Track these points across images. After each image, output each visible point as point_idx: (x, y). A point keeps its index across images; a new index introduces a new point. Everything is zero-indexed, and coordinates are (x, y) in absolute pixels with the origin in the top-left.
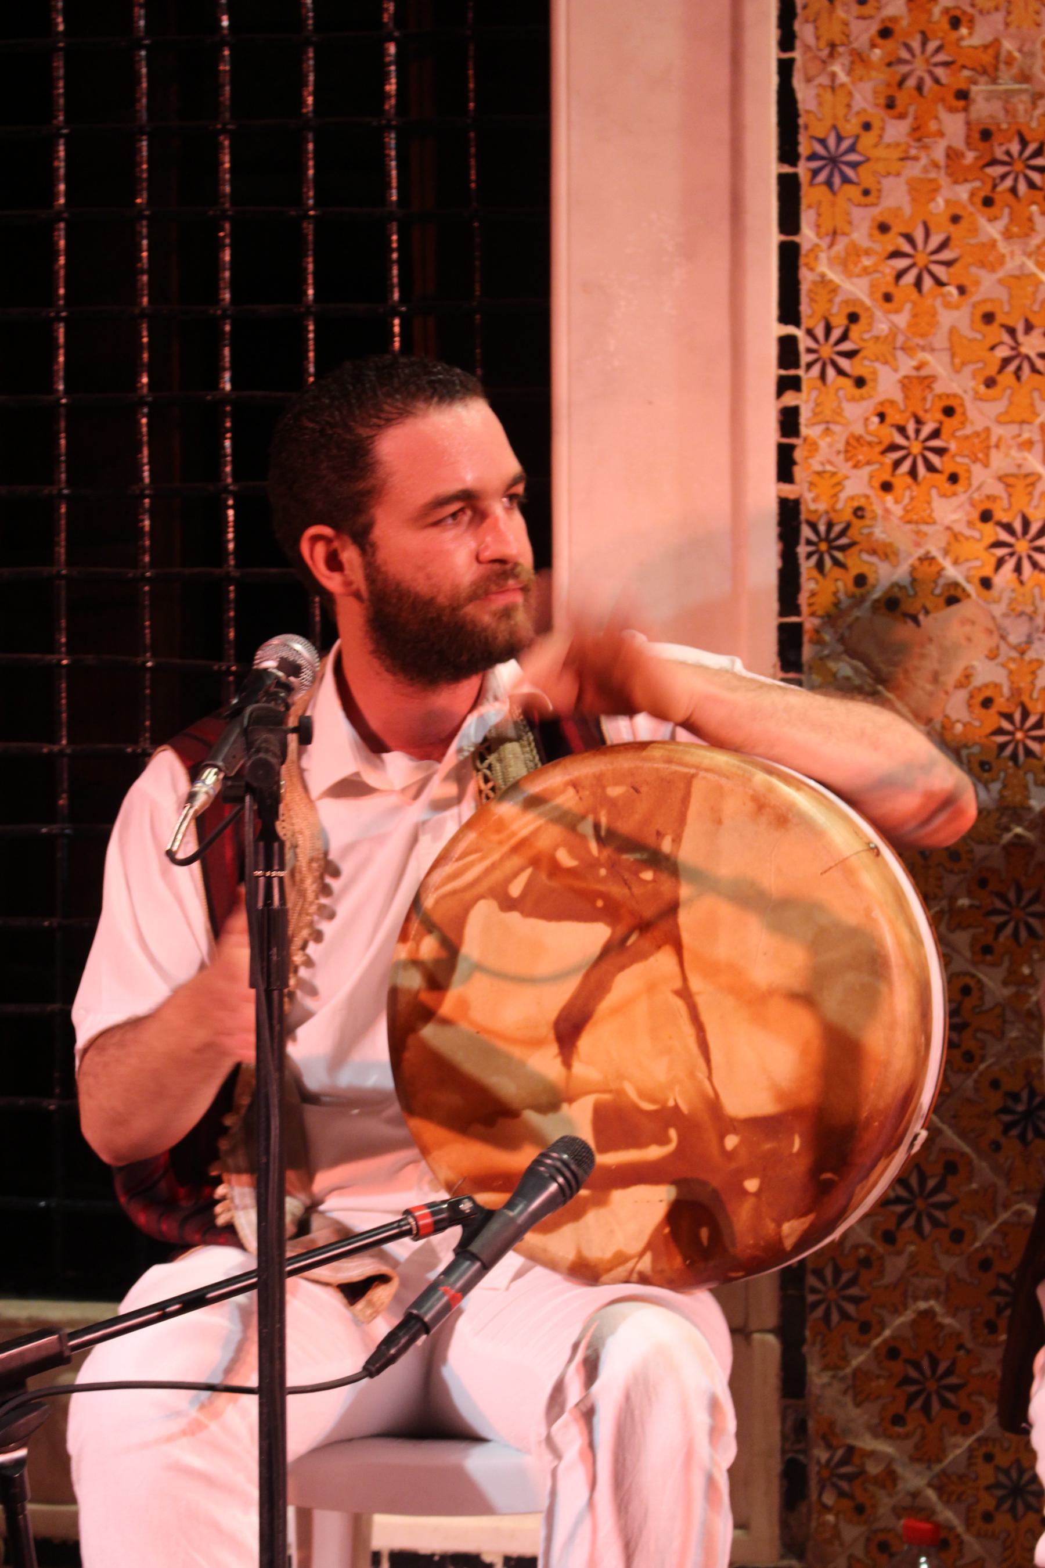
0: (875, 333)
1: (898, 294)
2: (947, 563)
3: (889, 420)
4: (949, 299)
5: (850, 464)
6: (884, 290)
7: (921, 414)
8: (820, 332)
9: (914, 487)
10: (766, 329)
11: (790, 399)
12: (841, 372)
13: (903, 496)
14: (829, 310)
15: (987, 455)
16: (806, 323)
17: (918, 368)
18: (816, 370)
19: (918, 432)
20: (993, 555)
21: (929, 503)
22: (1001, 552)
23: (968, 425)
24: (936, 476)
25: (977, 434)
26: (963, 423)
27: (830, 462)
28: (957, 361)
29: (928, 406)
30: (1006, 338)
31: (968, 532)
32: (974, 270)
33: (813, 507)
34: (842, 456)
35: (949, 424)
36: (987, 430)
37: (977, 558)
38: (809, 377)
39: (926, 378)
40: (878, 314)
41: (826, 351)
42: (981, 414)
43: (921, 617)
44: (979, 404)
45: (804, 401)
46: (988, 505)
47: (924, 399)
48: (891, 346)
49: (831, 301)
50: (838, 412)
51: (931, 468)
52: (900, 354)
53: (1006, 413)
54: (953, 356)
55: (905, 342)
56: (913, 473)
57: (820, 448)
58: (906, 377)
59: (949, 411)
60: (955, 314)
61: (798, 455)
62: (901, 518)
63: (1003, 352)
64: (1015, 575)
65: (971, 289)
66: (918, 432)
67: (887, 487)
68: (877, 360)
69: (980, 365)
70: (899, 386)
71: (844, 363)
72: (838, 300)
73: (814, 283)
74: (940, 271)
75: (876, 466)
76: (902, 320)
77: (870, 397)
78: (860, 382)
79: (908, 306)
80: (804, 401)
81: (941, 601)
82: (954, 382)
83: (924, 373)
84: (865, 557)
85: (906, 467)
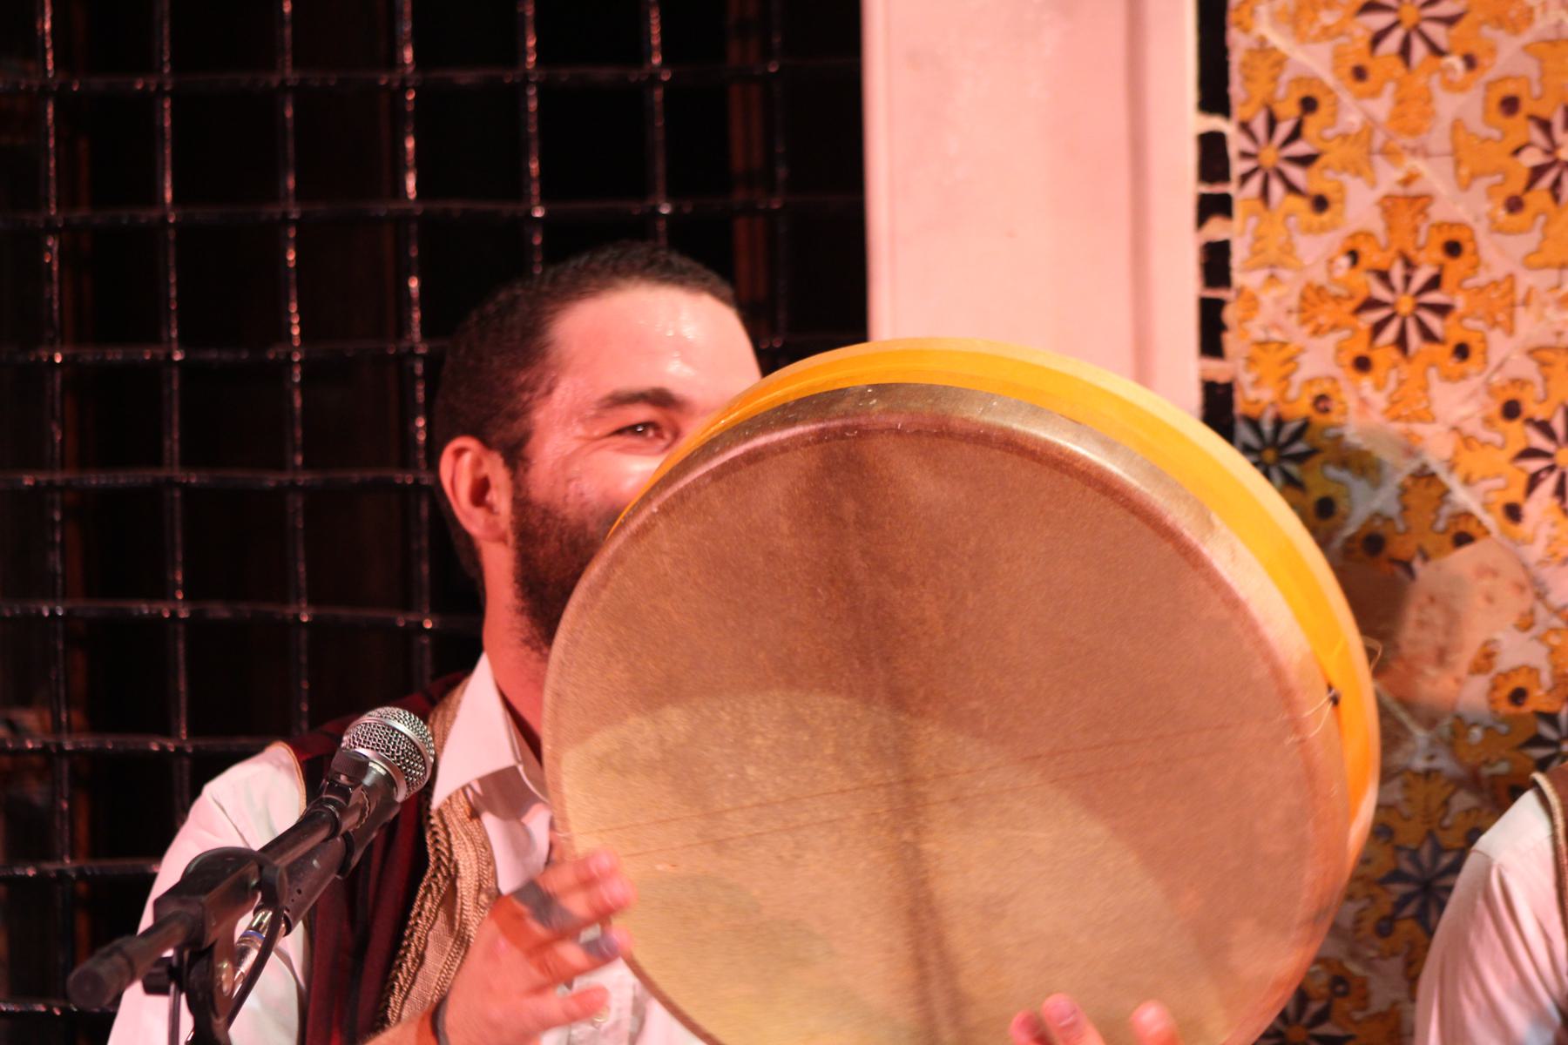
0: (1340, 128)
1: (1375, 70)
2: (1453, 482)
3: (1365, 262)
4: (1450, 76)
5: (1307, 329)
6: (1353, 61)
7: (1411, 252)
8: (1259, 126)
9: (1404, 367)
10: (1180, 121)
11: (1217, 229)
12: (1291, 188)
13: (1386, 378)
14: (1272, 93)
15: (1511, 317)
16: (1238, 111)
17: (1407, 182)
18: (1254, 184)
19: (1408, 279)
20: (1522, 470)
21: (1425, 388)
22: (1535, 465)
23: (1481, 269)
24: (1435, 348)
25: (1495, 284)
26: (1474, 267)
27: (1278, 327)
28: (1464, 171)
29: (1422, 239)
30: (1537, 136)
31: (1485, 435)
32: (1487, 31)
33: (1252, 394)
34: (1294, 319)
35: (1455, 267)
36: (1511, 277)
37: (1498, 476)
38: (1243, 195)
39: (1417, 198)
40: (1346, 98)
41: (1270, 156)
42: (1501, 254)
43: (1417, 565)
44: (1499, 238)
45: (1236, 231)
46: (1512, 394)
47: (1416, 230)
48: (1365, 149)
49: (1274, 79)
50: (1288, 249)
51: (1428, 335)
52: (1379, 161)
53: (1538, 251)
54: (1458, 163)
55: (1386, 143)
56: (1401, 342)
57: (1263, 303)
58: (1388, 197)
59: (1453, 249)
60: (1460, 99)
61: (1230, 315)
62: (1386, 412)
63: (1532, 158)
64: (1556, 502)
65: (1483, 61)
66: (1408, 279)
67: (1362, 364)
68: (1344, 169)
69: (1498, 178)
70: (1377, 211)
71: (1296, 174)
72: (1286, 77)
73: (1251, 51)
74: (1437, 32)
75: (1345, 333)
76: (1381, 107)
77: (1333, 226)
78: (1320, 203)
79: (1390, 88)
80: (1236, 231)
81: (1447, 539)
82: (1461, 204)
83: (1415, 189)
84: (1333, 472)
85: (1390, 333)
